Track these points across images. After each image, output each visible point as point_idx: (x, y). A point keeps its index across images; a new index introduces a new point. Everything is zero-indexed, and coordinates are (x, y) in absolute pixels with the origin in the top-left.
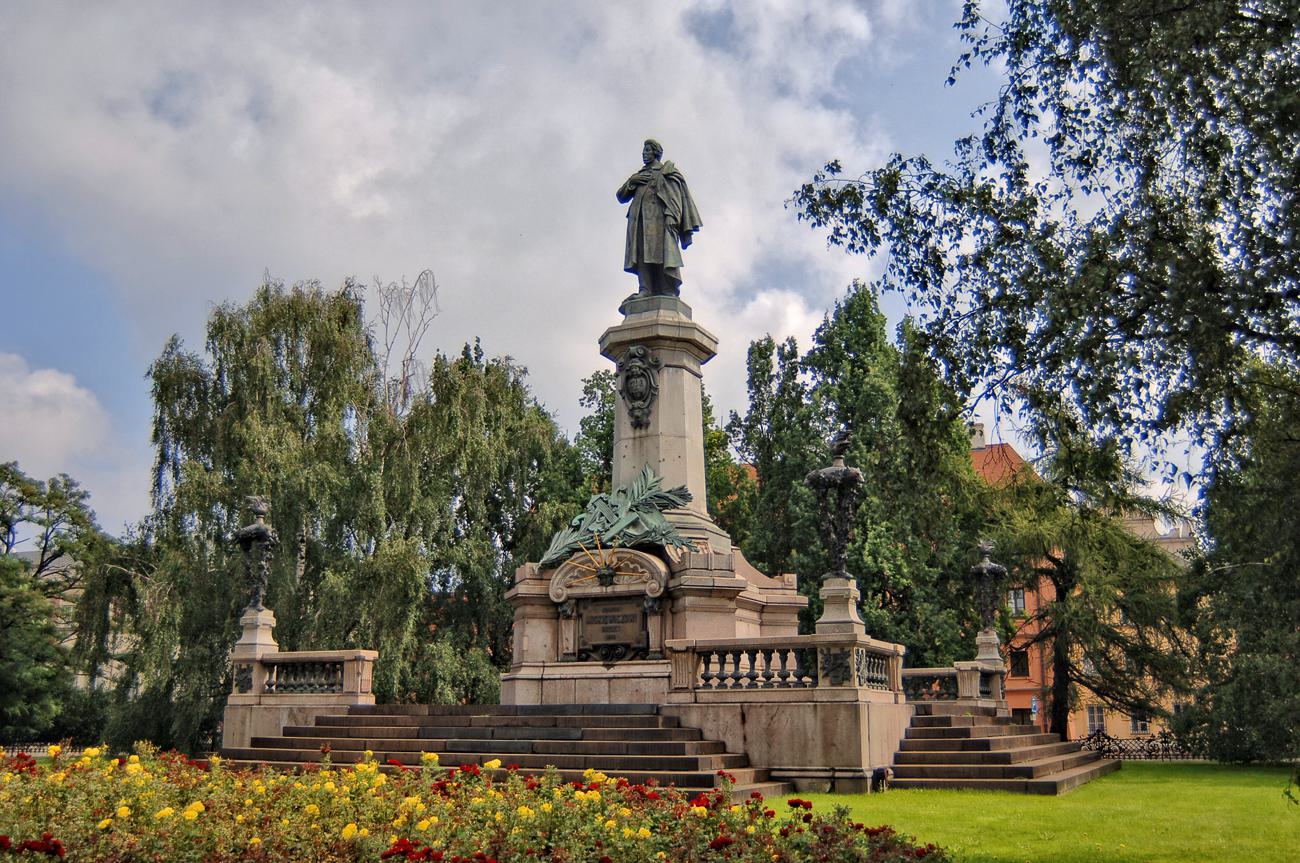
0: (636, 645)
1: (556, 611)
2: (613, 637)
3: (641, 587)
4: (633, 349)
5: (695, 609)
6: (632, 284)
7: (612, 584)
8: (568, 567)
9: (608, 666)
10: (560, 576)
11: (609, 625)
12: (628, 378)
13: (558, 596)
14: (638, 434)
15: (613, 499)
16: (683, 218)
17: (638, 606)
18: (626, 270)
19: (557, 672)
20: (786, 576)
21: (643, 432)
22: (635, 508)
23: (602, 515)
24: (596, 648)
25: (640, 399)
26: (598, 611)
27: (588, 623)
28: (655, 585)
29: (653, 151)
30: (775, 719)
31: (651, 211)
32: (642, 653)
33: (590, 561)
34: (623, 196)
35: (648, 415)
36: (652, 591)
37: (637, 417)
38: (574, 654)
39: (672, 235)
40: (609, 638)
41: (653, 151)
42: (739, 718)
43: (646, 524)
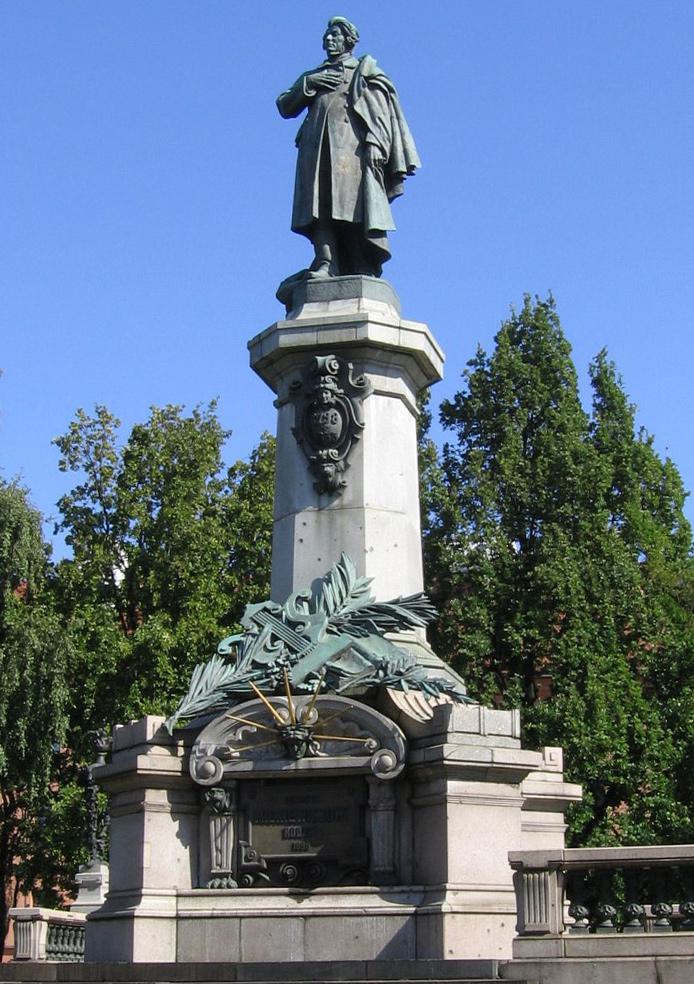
3: (360, 761)
5: (461, 799)
6: (300, 253)
9: (299, 896)
15: (289, 609)
16: (393, 148)
18: (296, 229)
19: (206, 906)
20: (548, 750)
28: (389, 760)
36: (382, 767)
37: (328, 475)
39: (377, 178)
41: (339, 39)
43: (365, 655)
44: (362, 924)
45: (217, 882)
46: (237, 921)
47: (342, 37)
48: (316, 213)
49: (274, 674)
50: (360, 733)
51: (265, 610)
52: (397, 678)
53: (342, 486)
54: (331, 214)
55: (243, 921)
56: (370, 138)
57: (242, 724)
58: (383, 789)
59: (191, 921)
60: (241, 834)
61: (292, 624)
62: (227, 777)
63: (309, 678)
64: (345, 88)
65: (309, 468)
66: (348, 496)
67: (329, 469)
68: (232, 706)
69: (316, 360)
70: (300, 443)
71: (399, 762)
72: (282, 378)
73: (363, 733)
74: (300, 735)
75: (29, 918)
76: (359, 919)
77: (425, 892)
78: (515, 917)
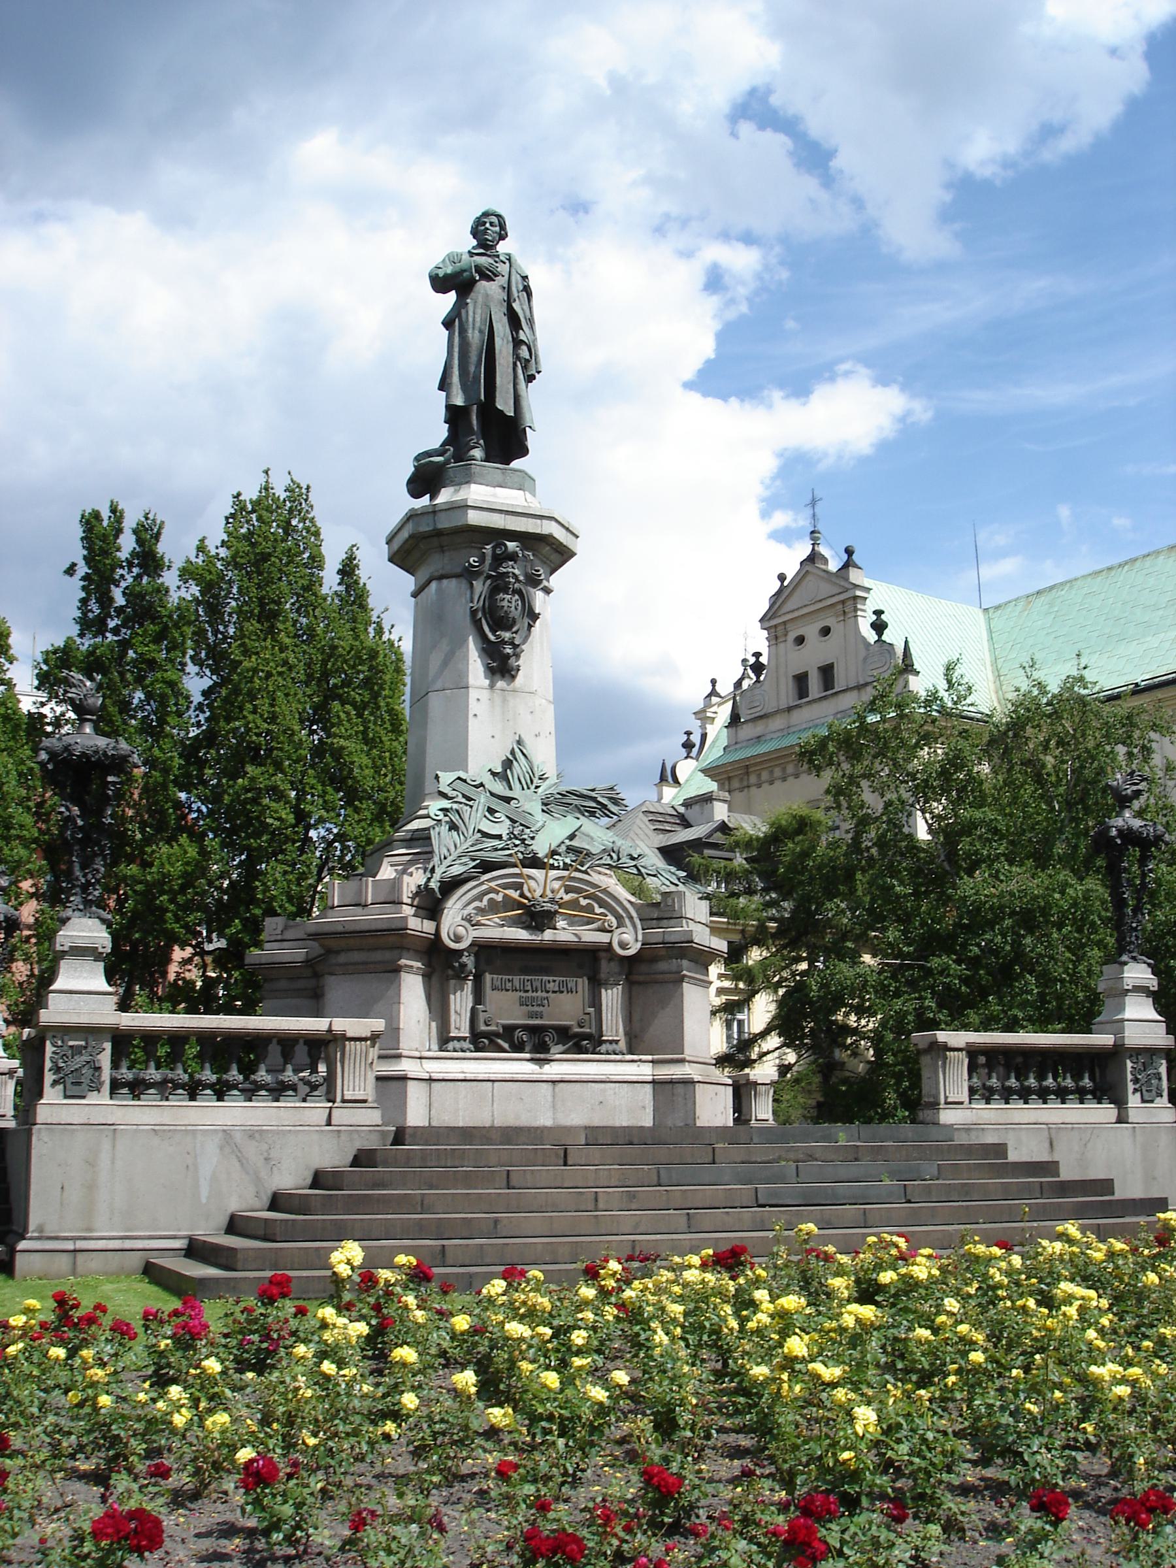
3: (604, 938)
4: (511, 545)
8: (475, 892)
10: (459, 905)
11: (530, 994)
12: (495, 590)
13: (458, 939)
23: (491, 811)
24: (509, 1030)
30: (1089, 1145)
32: (584, 1041)
33: (518, 887)
35: (518, 656)
36: (623, 945)
37: (508, 656)
38: (464, 1039)
40: (531, 1016)
42: (1047, 1145)
44: (604, 1090)
45: (457, 1044)
46: (490, 1084)
47: (497, 229)
48: (482, 398)
49: (516, 846)
50: (598, 910)
51: (459, 778)
52: (634, 863)
54: (494, 401)
55: (496, 1084)
56: (522, 336)
57: (491, 890)
58: (612, 964)
59: (444, 1083)
61: (508, 800)
62: (472, 944)
63: (554, 853)
64: (502, 281)
67: (508, 650)
68: (483, 873)
69: (505, 545)
71: (637, 940)
72: (443, 552)
73: (602, 910)
75: (6, 1071)
76: (603, 1085)
77: (652, 1062)
78: (731, 1088)
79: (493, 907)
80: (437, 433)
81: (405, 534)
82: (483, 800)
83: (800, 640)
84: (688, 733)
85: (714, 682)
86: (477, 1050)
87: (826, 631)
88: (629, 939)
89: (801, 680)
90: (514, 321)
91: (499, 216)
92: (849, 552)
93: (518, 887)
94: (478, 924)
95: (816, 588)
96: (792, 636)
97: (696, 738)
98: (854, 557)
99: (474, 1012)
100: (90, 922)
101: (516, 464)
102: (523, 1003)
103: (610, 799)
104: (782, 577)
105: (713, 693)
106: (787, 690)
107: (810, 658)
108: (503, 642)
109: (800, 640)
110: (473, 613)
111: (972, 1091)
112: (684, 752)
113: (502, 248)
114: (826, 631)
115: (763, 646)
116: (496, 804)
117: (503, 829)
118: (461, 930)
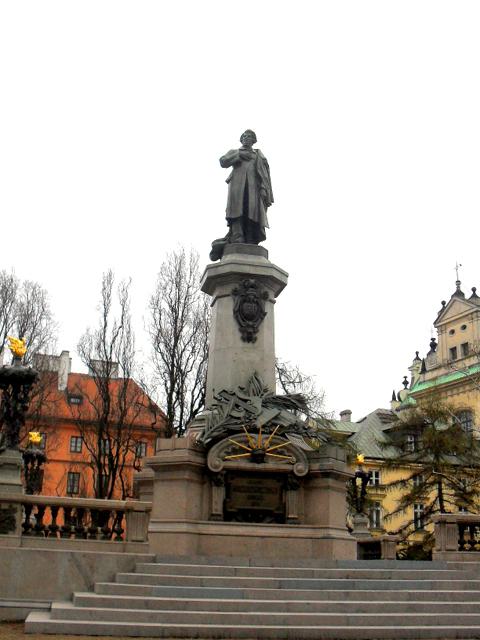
0: (276, 512)
1: (205, 476)
2: (258, 505)
3: (289, 467)
4: (252, 281)
5: (333, 489)
7: (263, 461)
8: (225, 444)
13: (216, 467)
14: (247, 345)
17: (279, 481)
18: (227, 219)
21: (250, 344)
22: (265, 404)
23: (237, 406)
25: (250, 320)
26: (243, 482)
27: (235, 490)
29: (249, 138)
31: (252, 182)
32: (280, 518)
33: (246, 442)
34: (225, 163)
35: (255, 332)
36: (298, 471)
37: (250, 333)
38: (219, 515)
41: (249, 138)
51: (224, 391)
53: (256, 339)
57: (233, 444)
60: (228, 495)
61: (246, 401)
62: (224, 469)
63: (264, 426)
65: (241, 331)
66: (256, 344)
67: (251, 330)
70: (236, 318)
74: (261, 452)
79: (235, 451)
80: (222, 230)
81: (205, 278)
82: (233, 400)
83: (453, 332)
84: (405, 377)
85: (417, 353)
86: (225, 520)
87: (464, 327)
88: (301, 469)
89: (453, 350)
90: (259, 179)
91: (253, 133)
92: (474, 290)
93: (246, 442)
94: (226, 460)
95: (461, 308)
96: (449, 330)
97: (409, 380)
98: (477, 293)
99: (225, 503)
100: (14, 452)
101: (260, 244)
102: (249, 498)
103: (298, 401)
104: (443, 303)
105: (417, 358)
106: (447, 355)
107: (457, 340)
108: (248, 326)
109: (453, 332)
110: (235, 312)
111: (462, 542)
112: (403, 386)
113: (254, 147)
114: (464, 327)
115: (435, 336)
116: (240, 403)
117: (241, 415)
118: (217, 463)
